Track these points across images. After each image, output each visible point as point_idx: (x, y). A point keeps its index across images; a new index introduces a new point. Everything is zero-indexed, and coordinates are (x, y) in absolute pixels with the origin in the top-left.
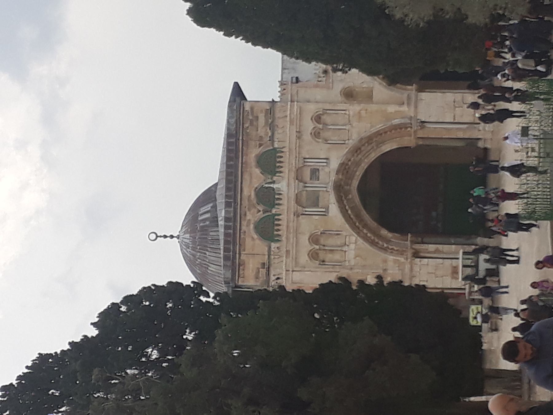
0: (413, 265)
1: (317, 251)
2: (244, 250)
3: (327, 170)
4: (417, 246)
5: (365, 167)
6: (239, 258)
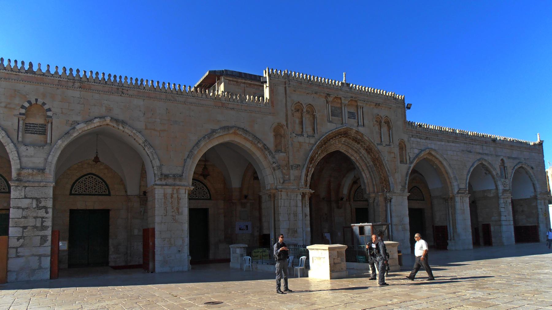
0: (296, 193)
1: (300, 112)
2: (247, 87)
3: (356, 125)
4: (307, 198)
5: (352, 158)
6: (241, 83)
